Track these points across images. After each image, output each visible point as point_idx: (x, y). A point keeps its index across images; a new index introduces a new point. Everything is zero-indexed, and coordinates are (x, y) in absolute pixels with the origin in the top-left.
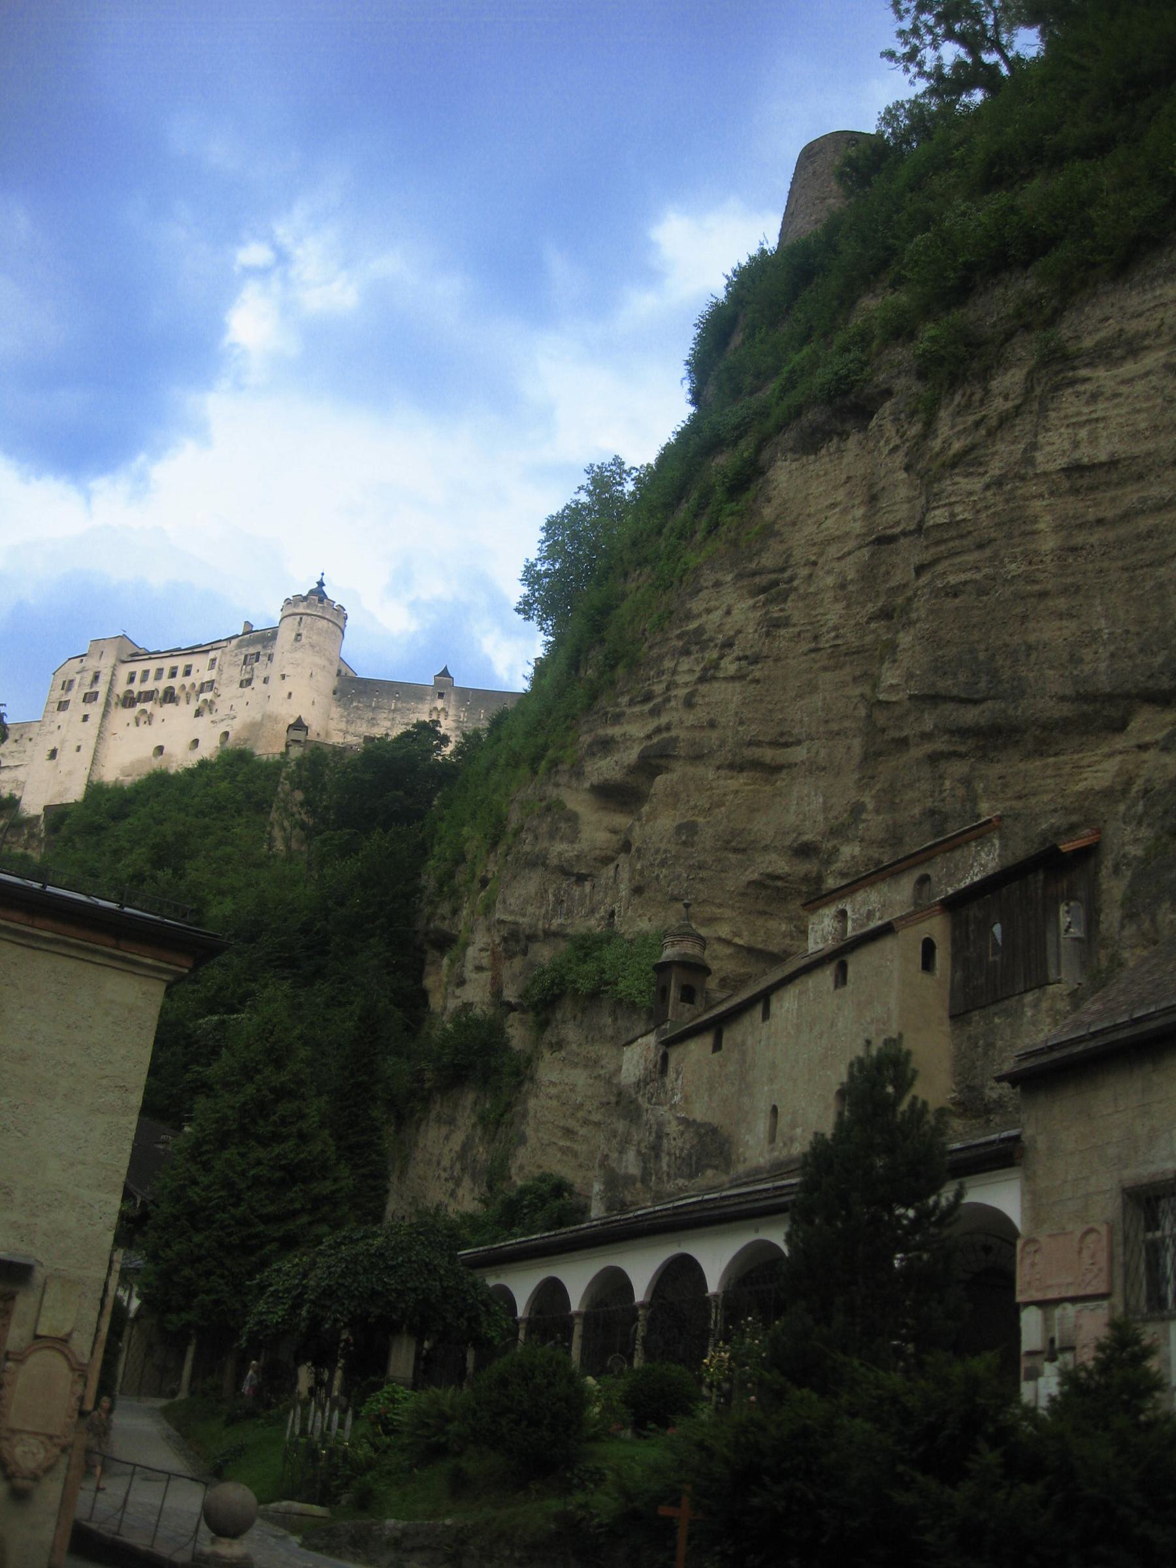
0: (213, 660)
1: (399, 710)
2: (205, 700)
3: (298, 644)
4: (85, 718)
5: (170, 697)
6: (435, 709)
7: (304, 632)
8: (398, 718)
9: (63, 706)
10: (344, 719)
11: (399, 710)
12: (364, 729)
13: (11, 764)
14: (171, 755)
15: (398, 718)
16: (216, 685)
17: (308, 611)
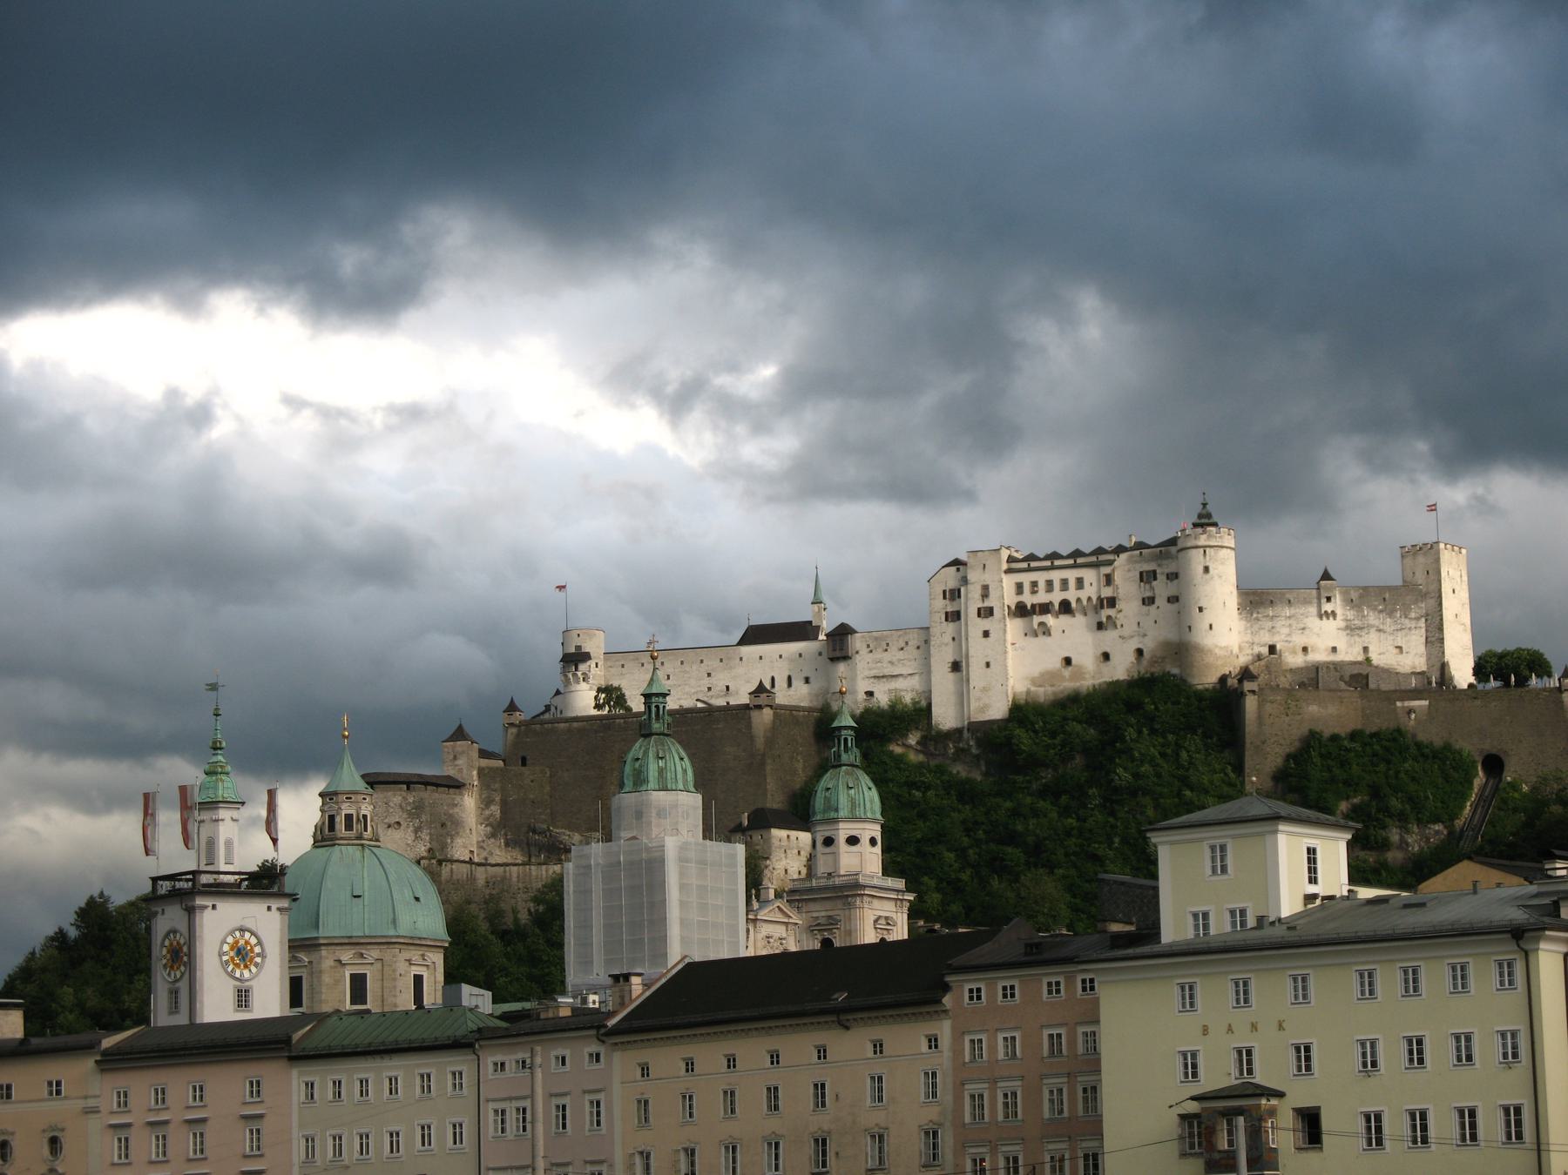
3: (1207, 576)
4: (986, 634)
5: (1065, 607)
6: (1326, 612)
10: (1249, 631)
12: (1268, 639)
14: (1080, 667)
15: (1291, 621)
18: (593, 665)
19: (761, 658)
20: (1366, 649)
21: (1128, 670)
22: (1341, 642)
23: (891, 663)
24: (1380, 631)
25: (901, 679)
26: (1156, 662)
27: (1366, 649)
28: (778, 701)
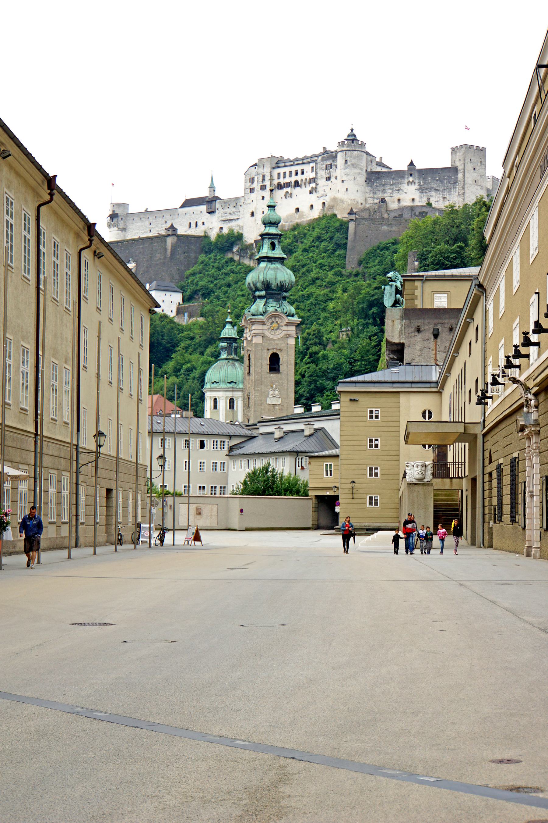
0: (313, 168)
1: (394, 184)
2: (312, 187)
3: (346, 165)
4: (263, 198)
5: (297, 184)
6: (409, 181)
7: (348, 159)
8: (394, 188)
9: (252, 190)
10: (372, 192)
11: (394, 184)
12: (380, 195)
13: (235, 218)
14: (303, 212)
16: (316, 180)
17: (349, 149)
18: (120, 219)
19: (186, 214)
20: (429, 199)
21: (320, 213)
22: (416, 195)
23: (230, 214)
24: (436, 190)
25: (234, 221)
26: (330, 208)
27: (429, 199)
28: (179, 233)
